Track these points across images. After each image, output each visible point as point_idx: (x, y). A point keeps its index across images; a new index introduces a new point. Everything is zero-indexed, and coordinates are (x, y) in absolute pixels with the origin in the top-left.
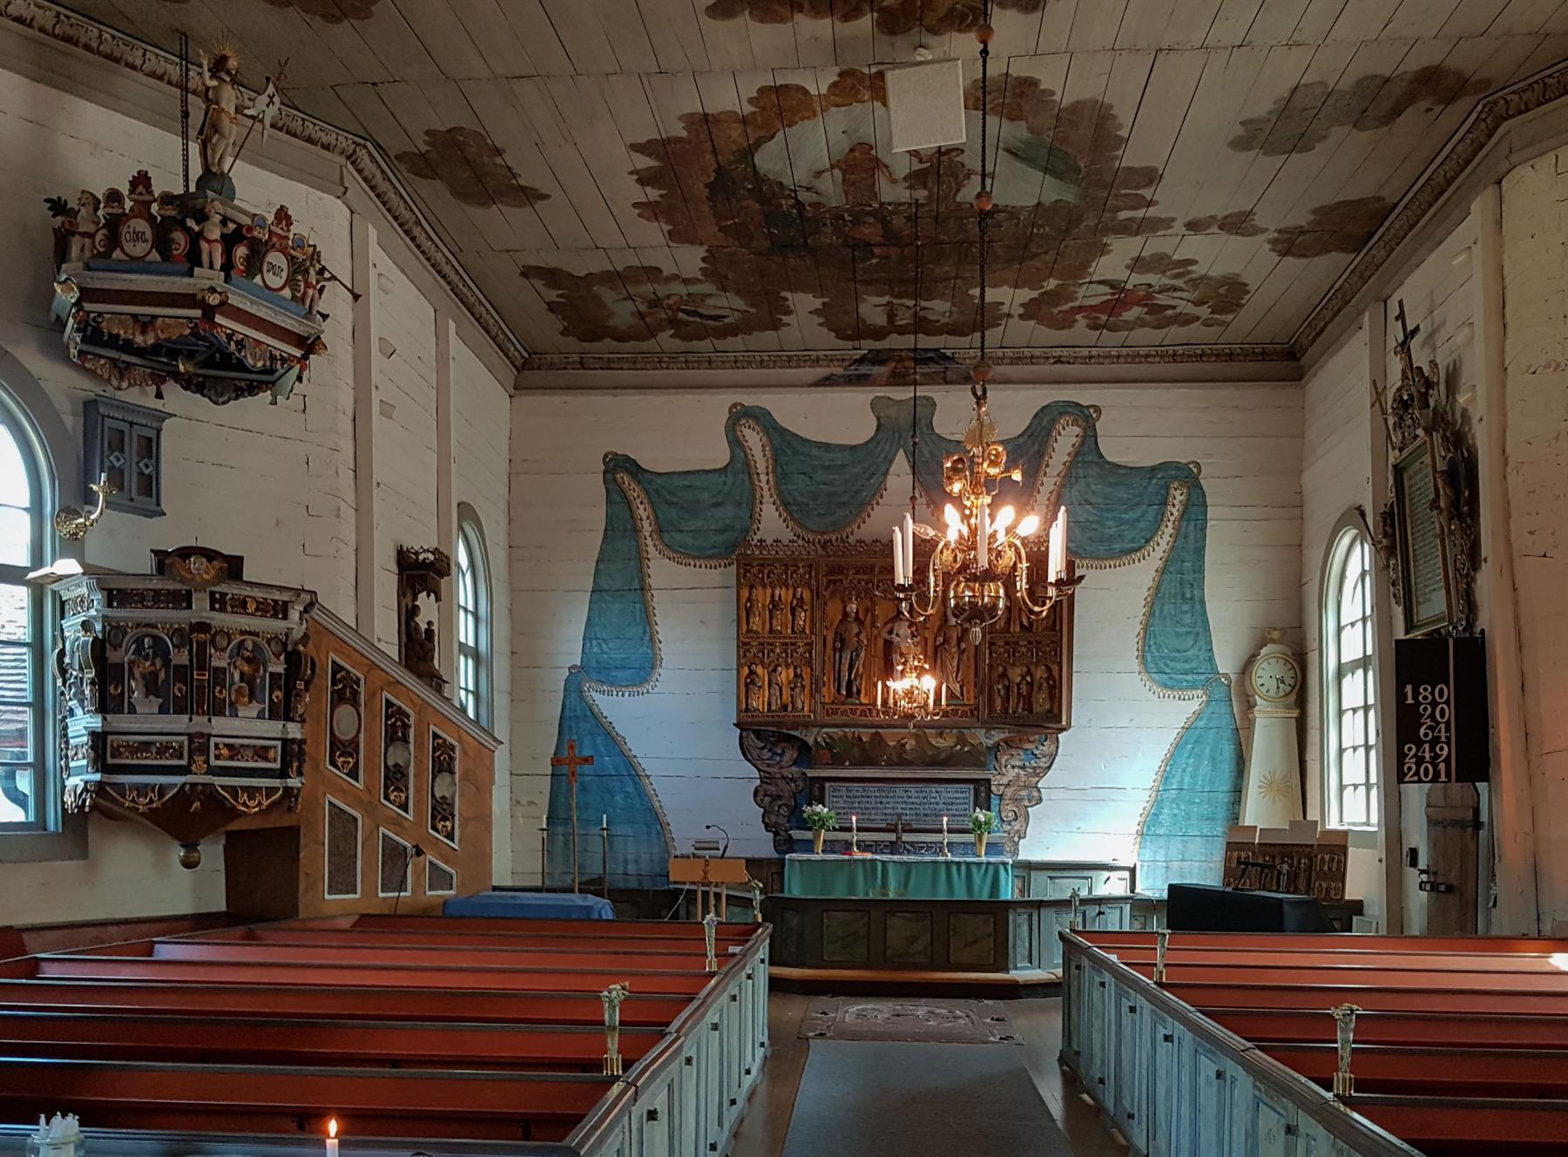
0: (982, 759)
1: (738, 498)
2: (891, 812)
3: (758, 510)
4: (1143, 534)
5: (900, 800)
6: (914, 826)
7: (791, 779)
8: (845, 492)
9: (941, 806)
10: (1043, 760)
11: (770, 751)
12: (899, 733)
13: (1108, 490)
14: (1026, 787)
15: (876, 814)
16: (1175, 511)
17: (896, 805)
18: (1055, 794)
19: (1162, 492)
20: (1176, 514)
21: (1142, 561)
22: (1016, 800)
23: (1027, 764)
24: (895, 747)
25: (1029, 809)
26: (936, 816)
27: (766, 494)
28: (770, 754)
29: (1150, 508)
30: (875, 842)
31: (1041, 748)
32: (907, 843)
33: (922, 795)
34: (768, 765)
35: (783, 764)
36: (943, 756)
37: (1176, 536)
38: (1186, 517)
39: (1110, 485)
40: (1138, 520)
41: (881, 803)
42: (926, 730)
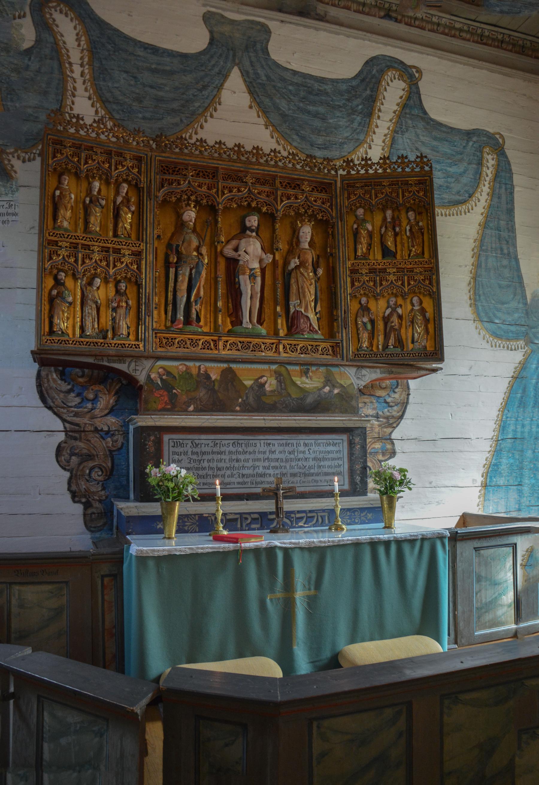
0: (354, 403)
1: (44, 85)
2: (250, 472)
3: (69, 102)
4: (466, 188)
5: (261, 456)
8: (174, 99)
9: (311, 463)
13: (435, 143)
15: (232, 476)
16: (489, 172)
17: (257, 463)
19: (478, 154)
20: (490, 175)
21: (467, 213)
24: (252, 387)
26: (305, 475)
27: (79, 85)
29: (470, 166)
33: (287, 449)
36: (310, 400)
37: (492, 194)
38: (498, 179)
39: (435, 139)
40: (461, 175)
41: (238, 461)
42: (290, 368)
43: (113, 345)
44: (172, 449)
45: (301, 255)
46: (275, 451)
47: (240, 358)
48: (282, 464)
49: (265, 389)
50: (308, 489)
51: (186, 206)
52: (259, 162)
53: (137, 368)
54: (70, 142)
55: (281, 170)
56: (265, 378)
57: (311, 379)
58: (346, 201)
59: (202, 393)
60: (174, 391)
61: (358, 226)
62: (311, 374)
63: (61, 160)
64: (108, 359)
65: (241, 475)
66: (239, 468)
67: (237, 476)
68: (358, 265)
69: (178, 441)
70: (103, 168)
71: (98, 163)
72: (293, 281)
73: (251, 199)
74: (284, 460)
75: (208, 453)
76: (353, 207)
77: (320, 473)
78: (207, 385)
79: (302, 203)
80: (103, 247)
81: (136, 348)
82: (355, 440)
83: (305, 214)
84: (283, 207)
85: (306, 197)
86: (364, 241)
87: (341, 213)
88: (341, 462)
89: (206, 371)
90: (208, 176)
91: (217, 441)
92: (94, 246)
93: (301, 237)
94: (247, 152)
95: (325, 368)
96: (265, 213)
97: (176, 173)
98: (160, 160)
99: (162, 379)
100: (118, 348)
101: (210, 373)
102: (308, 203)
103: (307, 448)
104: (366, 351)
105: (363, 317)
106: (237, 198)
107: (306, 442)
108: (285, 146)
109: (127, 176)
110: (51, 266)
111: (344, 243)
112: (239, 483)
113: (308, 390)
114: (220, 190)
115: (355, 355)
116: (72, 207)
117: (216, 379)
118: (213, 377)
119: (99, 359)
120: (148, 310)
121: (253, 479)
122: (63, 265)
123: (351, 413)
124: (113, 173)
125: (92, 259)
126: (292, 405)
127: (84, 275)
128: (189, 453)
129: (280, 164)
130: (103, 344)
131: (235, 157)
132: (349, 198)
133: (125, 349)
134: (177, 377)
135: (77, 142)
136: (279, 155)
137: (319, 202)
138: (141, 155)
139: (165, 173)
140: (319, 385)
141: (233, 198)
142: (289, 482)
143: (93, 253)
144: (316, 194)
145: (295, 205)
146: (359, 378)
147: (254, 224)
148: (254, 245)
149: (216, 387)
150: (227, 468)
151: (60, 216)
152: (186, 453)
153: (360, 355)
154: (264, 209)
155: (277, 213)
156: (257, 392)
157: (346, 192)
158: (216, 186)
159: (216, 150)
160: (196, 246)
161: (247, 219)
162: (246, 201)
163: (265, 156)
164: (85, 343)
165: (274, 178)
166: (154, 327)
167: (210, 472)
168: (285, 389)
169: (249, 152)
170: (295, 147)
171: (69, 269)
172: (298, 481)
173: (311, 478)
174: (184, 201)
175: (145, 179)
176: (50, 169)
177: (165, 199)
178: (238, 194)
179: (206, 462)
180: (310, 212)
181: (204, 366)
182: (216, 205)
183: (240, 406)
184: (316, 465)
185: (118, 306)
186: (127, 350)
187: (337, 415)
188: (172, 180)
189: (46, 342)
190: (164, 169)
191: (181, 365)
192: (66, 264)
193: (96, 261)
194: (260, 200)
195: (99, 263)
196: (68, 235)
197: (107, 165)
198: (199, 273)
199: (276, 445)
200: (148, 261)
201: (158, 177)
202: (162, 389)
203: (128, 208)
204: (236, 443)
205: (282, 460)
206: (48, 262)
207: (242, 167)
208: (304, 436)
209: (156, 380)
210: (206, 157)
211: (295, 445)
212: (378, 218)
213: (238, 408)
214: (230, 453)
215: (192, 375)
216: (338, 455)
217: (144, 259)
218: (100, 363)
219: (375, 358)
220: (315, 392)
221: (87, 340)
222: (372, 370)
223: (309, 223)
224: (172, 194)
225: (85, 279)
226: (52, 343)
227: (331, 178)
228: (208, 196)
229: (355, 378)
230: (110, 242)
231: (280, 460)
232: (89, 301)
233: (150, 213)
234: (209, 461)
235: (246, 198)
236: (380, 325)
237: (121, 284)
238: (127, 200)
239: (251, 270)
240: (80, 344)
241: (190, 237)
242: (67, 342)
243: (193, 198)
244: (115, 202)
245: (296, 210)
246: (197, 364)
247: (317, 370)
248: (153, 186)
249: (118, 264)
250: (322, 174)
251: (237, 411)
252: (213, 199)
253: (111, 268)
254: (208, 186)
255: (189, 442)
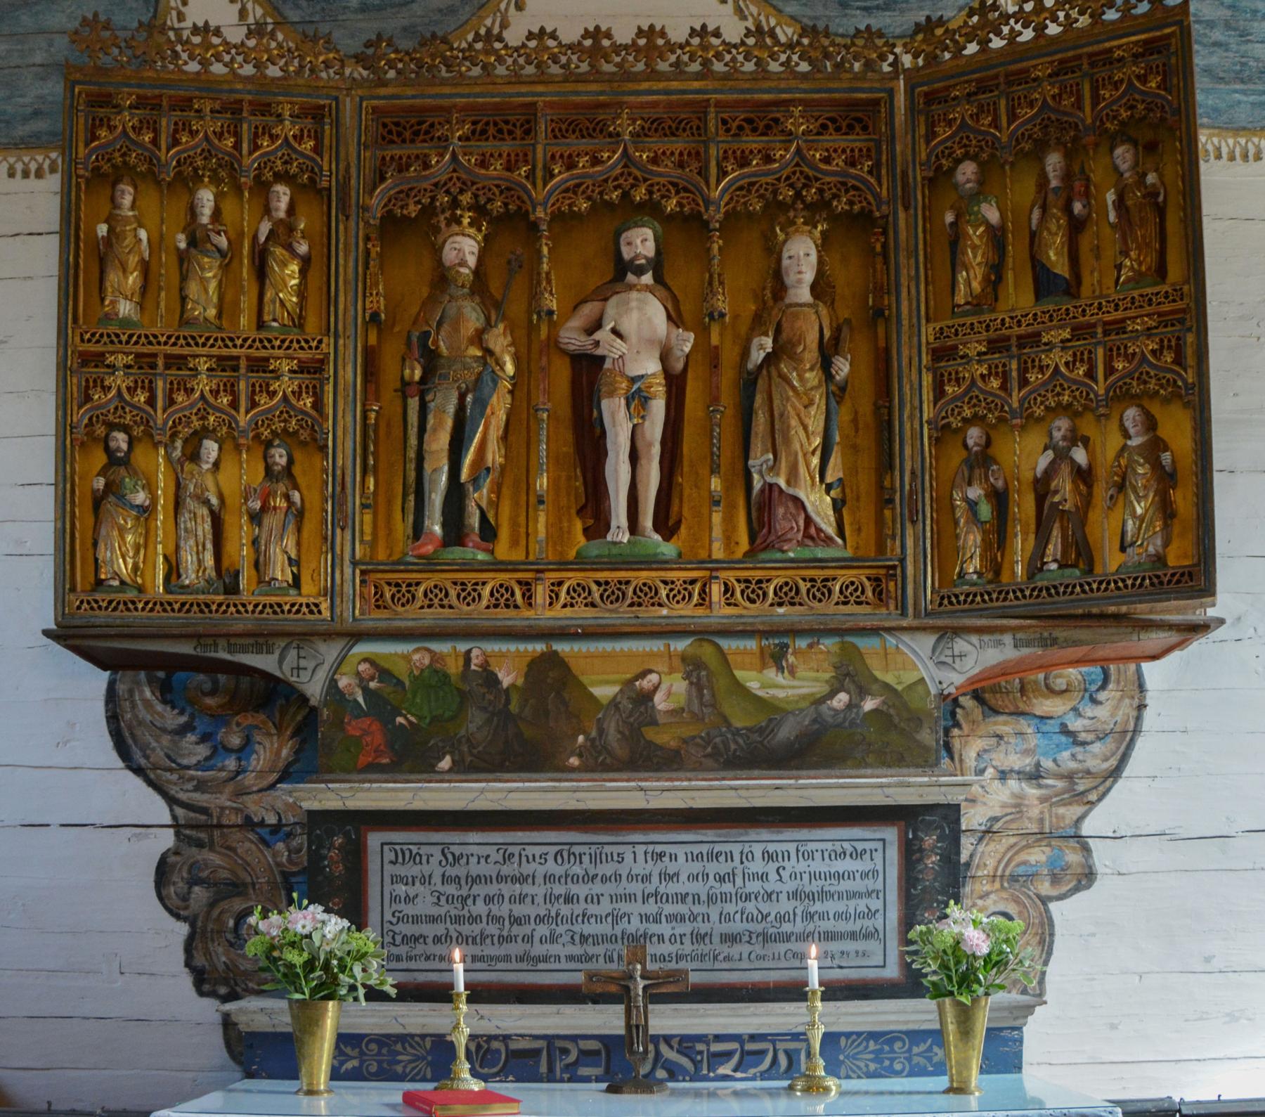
2: (605, 928)
5: (636, 888)
6: (694, 978)
7: (276, 829)
9: (785, 906)
10: (1097, 748)
11: (204, 738)
12: (631, 655)
14: (1043, 836)
15: (553, 939)
17: (624, 907)
18: (1135, 856)
22: (1014, 878)
23: (1047, 764)
24: (614, 703)
25: (1053, 906)
26: (766, 938)
28: (203, 751)
30: (550, 1039)
31: (1089, 711)
32: (667, 1039)
33: (713, 868)
34: (201, 786)
35: (249, 779)
36: (786, 732)
41: (569, 899)
42: (725, 644)
43: (250, 608)
44: (389, 868)
45: (785, 325)
46: (677, 875)
47: (579, 626)
48: (697, 909)
49: (653, 707)
50: (773, 977)
51: (448, 225)
52: (653, 71)
53: (303, 663)
54: (130, 94)
55: (717, 85)
56: (653, 678)
57: (792, 672)
58: (923, 147)
59: (474, 722)
60: (400, 720)
61: (958, 217)
62: (791, 659)
63: (109, 144)
64: (229, 645)
65: (577, 938)
66: (572, 919)
67: (567, 938)
68: (956, 334)
69: (405, 847)
70: (218, 149)
71: (206, 137)
72: (759, 400)
73: (631, 181)
74: (704, 898)
75: (488, 880)
76: (944, 162)
77: (811, 934)
78: (490, 702)
79: (785, 174)
80: (220, 358)
81: (311, 612)
82: (922, 840)
83: (794, 203)
84: (725, 190)
85: (799, 151)
86: (976, 259)
87: (905, 185)
88: (876, 904)
89: (485, 665)
90: (510, 132)
91: (511, 849)
92: (198, 356)
93: (787, 273)
94: (617, 49)
95: (837, 639)
96: (671, 217)
97: (421, 137)
98: (375, 109)
99: (366, 691)
100: (264, 615)
101: (496, 670)
102: (806, 169)
103: (772, 867)
104: (975, 584)
105: (970, 484)
106: (589, 182)
107: (771, 848)
108: (762, 18)
109: (286, 163)
110: (90, 419)
111: (913, 273)
112: (571, 958)
113: (782, 705)
114: (540, 165)
115: (942, 598)
116: (142, 261)
117: (513, 685)
118: (506, 680)
119: (206, 645)
120: (342, 512)
121: (611, 947)
122: (120, 412)
123: (917, 766)
124: (246, 161)
125: (193, 390)
126: (733, 747)
127: (174, 436)
128: (437, 879)
129: (718, 67)
130: (224, 608)
131: (585, 67)
132: (931, 135)
133: (281, 616)
134: (407, 683)
135: (149, 93)
136: (715, 41)
137: (839, 162)
138: (322, 102)
139: (392, 142)
140: (820, 689)
141: (578, 186)
142: (715, 958)
143: (195, 376)
144: (833, 140)
145: (763, 180)
146: (944, 663)
147: (640, 250)
148: (639, 309)
149: (514, 707)
150: (540, 919)
151: (110, 290)
152: (426, 880)
153: (957, 596)
154: (671, 205)
155: (707, 210)
156: (630, 716)
157: (922, 119)
158: (530, 157)
159: (528, 56)
160: (476, 330)
161: (624, 237)
162: (616, 188)
163: (673, 52)
164: (176, 607)
165: (701, 108)
166: (358, 555)
167: (493, 929)
168: (713, 706)
169: (626, 47)
170: (792, 17)
171: (135, 422)
172: (745, 956)
173: (782, 948)
174: (443, 211)
175: (334, 166)
176: (81, 172)
177: (390, 212)
178: (591, 170)
179: (480, 902)
180: (811, 194)
181: (479, 650)
182: (530, 209)
183: (580, 756)
184: (799, 912)
185: (265, 508)
186: (286, 620)
187: (869, 771)
188: (409, 157)
189: (79, 608)
190: (390, 132)
191: (417, 650)
192: (127, 409)
193: (202, 396)
194: (657, 179)
195: (211, 399)
196: (131, 336)
197: (230, 142)
198: (482, 404)
199: (682, 858)
200: (341, 381)
201: (368, 154)
202: (366, 715)
203: (289, 248)
204: (565, 854)
205: (697, 899)
206: (80, 407)
207: (602, 93)
208: (765, 834)
209: (352, 694)
210: (499, 80)
211: (737, 857)
212: (1023, 190)
213: (574, 761)
214: (548, 878)
215: (446, 676)
216: (870, 884)
217: (331, 380)
218: (208, 654)
219: (1000, 604)
220: (801, 710)
221: (183, 598)
222: (986, 638)
223: (808, 228)
224: (408, 196)
225: (179, 444)
226: (92, 608)
227: (877, 85)
228: (508, 189)
229: (930, 664)
230: (239, 342)
231: (690, 899)
232: (188, 500)
233: (346, 256)
234: (489, 899)
235: (616, 179)
236: (1024, 507)
237: (273, 451)
238: (284, 233)
239: (633, 380)
240: (165, 610)
241: (459, 308)
242: (130, 606)
243: (466, 199)
244: (255, 237)
245: (769, 195)
246: (462, 647)
247: (811, 646)
248: (353, 182)
249: (263, 399)
250: (848, 76)
251: (572, 769)
252: (522, 193)
253: (242, 410)
254: (509, 161)
255: (436, 851)
